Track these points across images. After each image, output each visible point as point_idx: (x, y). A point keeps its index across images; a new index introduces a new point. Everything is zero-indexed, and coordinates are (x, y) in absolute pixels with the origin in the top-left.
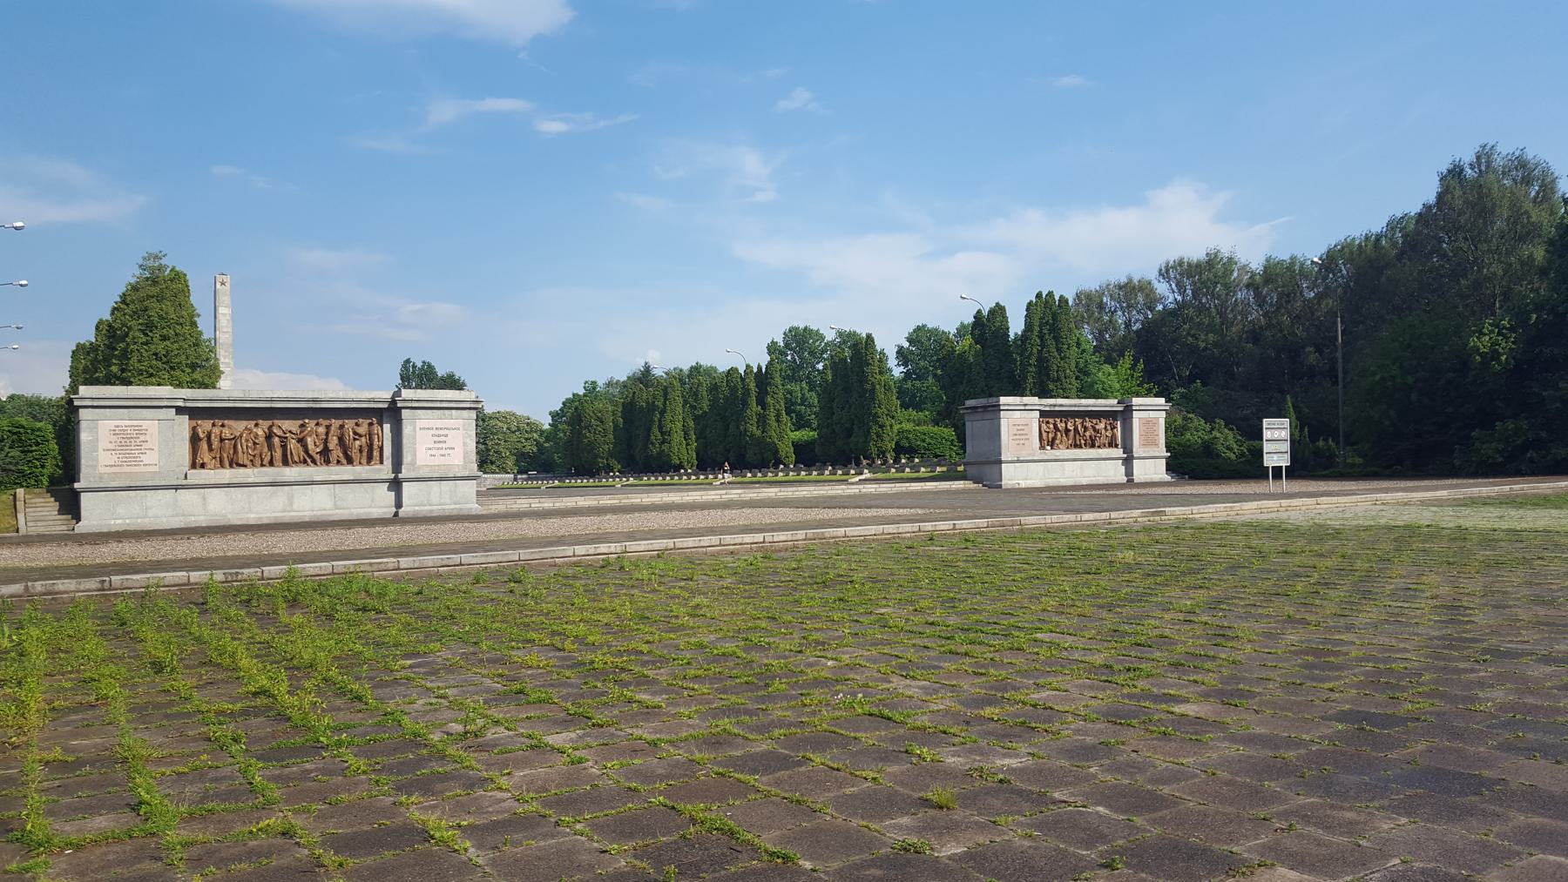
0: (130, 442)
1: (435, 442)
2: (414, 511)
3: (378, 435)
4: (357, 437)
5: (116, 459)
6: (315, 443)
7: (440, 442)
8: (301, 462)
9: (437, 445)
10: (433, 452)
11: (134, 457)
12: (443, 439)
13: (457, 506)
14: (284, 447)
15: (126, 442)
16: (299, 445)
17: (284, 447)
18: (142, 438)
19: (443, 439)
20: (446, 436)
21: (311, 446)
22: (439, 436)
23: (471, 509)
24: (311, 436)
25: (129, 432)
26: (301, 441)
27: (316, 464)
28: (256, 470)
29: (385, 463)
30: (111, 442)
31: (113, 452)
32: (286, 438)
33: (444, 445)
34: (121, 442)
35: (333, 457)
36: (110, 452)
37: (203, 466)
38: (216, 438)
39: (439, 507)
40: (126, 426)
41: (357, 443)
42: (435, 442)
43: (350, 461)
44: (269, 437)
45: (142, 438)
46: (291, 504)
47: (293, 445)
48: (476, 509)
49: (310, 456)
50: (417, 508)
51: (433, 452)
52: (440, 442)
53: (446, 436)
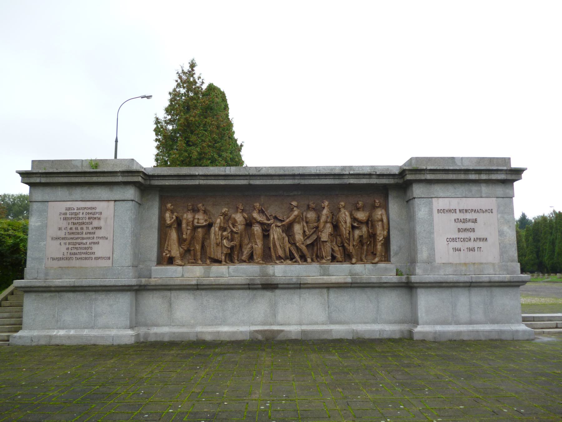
0: (82, 229)
1: (459, 230)
2: (435, 333)
3: (382, 220)
4: (355, 224)
5: (66, 251)
6: (304, 232)
7: (466, 230)
8: (286, 258)
9: (463, 235)
10: (458, 245)
11: (85, 248)
12: (470, 225)
13: (496, 327)
14: (266, 236)
15: (76, 229)
16: (284, 235)
17: (266, 236)
18: (96, 223)
19: (470, 225)
20: (475, 221)
21: (299, 237)
22: (465, 221)
23: (517, 331)
24: (299, 223)
25: (81, 216)
26: (288, 229)
27: (306, 261)
28: (232, 267)
29: (392, 259)
30: (60, 229)
31: (63, 242)
32: (269, 225)
33: (472, 235)
34: (71, 229)
35: (326, 250)
36: (59, 241)
37: (171, 261)
38: (187, 225)
39: (471, 328)
40: (78, 209)
41: (357, 233)
42: (459, 230)
43: (348, 257)
44: (249, 224)
45: (96, 223)
46: (275, 315)
47: (276, 234)
48: (524, 332)
49: (298, 249)
50: (439, 328)
51: (458, 245)
52: (466, 230)
53: (475, 221)
